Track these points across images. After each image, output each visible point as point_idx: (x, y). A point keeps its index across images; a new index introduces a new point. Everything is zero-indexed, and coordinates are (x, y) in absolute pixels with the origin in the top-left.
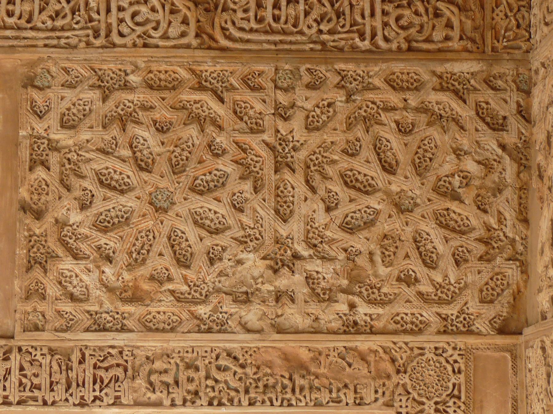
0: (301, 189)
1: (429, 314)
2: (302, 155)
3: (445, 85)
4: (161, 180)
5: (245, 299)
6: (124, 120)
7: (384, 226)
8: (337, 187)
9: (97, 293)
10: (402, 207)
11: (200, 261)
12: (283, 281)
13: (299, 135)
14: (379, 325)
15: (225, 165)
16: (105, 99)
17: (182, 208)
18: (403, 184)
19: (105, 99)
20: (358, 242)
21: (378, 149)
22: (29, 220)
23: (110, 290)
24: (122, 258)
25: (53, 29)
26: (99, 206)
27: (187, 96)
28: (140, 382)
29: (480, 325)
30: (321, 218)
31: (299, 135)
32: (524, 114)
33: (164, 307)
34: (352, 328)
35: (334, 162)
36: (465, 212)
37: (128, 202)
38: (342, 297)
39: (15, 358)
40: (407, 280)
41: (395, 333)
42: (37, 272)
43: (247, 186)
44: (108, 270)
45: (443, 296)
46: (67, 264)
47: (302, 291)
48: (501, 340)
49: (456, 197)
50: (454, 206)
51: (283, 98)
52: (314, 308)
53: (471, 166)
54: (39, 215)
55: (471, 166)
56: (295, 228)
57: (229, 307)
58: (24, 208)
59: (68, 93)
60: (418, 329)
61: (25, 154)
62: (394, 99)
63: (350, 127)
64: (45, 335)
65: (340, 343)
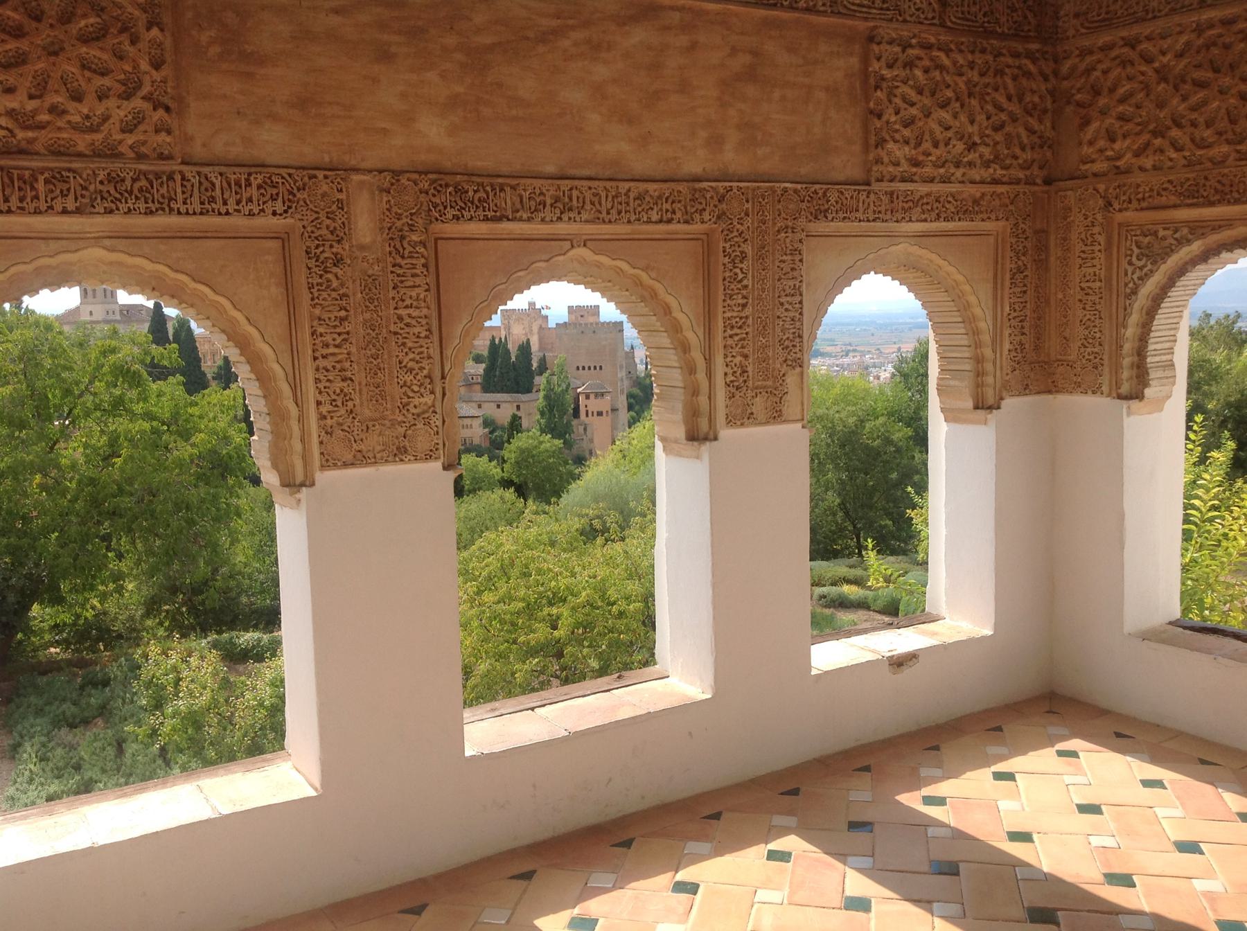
0: (978, 108)
1: (1021, 175)
2: (977, 89)
3: (1030, 56)
4: (927, 101)
5: (957, 165)
6: (909, 65)
7: (1007, 129)
8: (989, 107)
9: (903, 161)
10: (1014, 120)
11: (941, 145)
12: (971, 156)
13: (976, 78)
14: (1004, 180)
16: (903, 51)
17: (934, 116)
18: (1014, 108)
19: (903, 51)
20: (999, 137)
21: (1006, 88)
22: (876, 120)
23: (907, 160)
24: (913, 142)
25: (882, 9)
26: (902, 113)
27: (935, 53)
28: (919, 209)
29: (1039, 181)
30: (985, 123)
31: (976, 78)
32: (1056, 74)
33: (928, 170)
34: (995, 182)
35: (988, 94)
36: (1033, 122)
37: (914, 111)
38: (993, 165)
39: (872, 196)
40: (1016, 158)
41: (1010, 183)
42: (880, 149)
43: (958, 105)
44: (907, 149)
45: (1026, 166)
46: (890, 145)
48: (1046, 188)
49: (1031, 115)
50: (1030, 119)
51: (970, 57)
52: (982, 171)
53: (1036, 99)
54: (879, 116)
55: (1036, 99)
56: (976, 127)
57: (952, 170)
58: (871, 112)
59: (888, 47)
60: (1018, 182)
61: (872, 81)
62: (1010, 61)
63: (995, 75)
64: (885, 184)
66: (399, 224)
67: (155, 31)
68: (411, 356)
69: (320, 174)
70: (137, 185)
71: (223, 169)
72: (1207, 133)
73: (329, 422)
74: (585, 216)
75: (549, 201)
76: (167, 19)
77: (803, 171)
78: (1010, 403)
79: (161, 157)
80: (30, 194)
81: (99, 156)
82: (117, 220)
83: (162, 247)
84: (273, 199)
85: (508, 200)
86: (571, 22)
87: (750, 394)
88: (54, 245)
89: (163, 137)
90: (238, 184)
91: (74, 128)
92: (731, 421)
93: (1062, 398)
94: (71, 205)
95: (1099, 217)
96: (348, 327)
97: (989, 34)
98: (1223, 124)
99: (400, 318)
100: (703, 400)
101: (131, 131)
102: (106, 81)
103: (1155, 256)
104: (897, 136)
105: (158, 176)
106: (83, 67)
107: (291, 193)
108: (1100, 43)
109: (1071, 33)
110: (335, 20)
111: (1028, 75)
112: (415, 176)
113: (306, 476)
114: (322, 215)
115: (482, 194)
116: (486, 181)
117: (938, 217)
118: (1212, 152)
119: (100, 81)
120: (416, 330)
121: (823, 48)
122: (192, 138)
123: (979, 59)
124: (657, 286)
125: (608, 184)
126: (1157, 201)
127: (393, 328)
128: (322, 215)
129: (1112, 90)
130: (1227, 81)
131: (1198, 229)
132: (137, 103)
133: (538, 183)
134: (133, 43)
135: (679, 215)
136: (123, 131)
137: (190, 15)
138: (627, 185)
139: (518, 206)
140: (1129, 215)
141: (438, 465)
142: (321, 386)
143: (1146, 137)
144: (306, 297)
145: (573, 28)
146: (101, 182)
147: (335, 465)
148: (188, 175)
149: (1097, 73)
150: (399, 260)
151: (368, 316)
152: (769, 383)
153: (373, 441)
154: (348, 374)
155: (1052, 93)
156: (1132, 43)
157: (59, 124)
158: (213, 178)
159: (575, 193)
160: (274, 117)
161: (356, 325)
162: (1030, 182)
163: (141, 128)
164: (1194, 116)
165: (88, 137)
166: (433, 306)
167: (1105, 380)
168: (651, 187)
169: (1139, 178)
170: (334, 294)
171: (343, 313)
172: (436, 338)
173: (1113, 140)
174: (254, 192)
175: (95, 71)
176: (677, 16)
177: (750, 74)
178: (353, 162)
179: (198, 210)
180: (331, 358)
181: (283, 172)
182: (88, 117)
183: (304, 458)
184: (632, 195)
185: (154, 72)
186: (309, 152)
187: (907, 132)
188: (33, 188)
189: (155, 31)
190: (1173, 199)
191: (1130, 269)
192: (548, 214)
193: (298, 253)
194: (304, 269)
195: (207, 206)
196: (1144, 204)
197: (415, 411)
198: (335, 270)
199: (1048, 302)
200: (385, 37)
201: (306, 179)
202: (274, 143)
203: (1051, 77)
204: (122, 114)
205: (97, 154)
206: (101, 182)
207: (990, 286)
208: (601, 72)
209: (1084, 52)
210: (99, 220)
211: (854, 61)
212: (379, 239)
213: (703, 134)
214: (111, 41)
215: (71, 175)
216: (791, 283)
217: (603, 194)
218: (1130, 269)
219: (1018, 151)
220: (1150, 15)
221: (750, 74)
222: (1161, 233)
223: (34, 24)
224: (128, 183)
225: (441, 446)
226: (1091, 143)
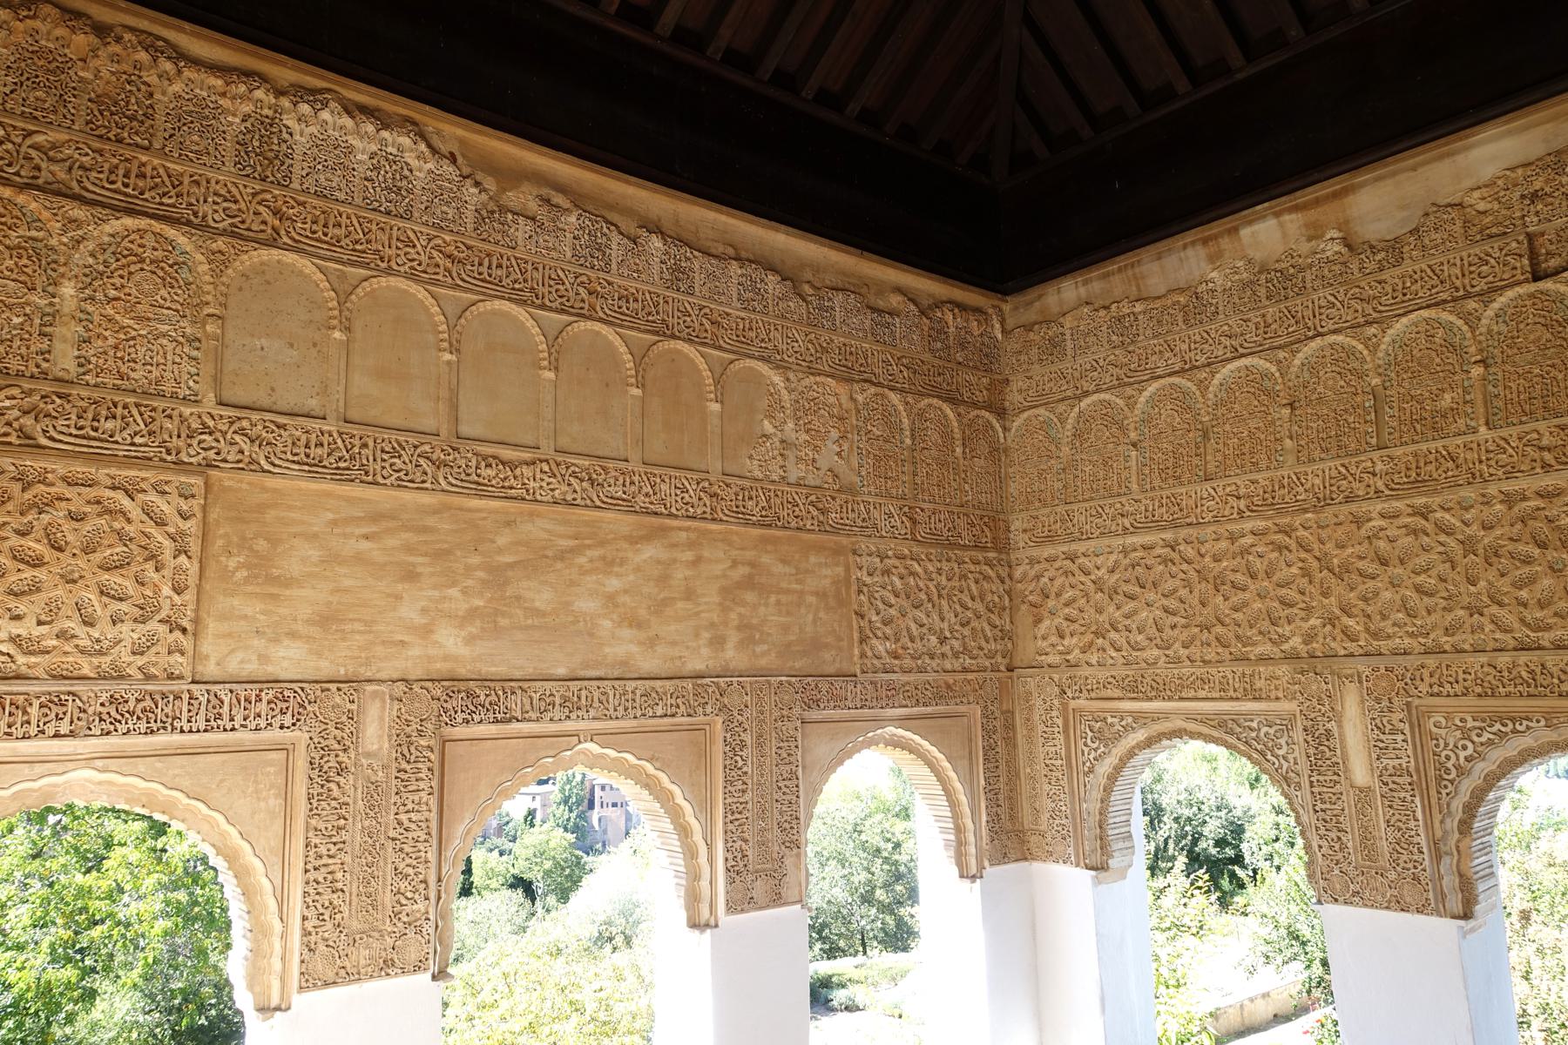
13: (944, 581)
15: (924, 597)
20: (966, 631)
27: (909, 562)
30: (953, 620)
31: (944, 581)
33: (908, 662)
34: (965, 670)
40: (981, 648)
45: (991, 655)
46: (874, 641)
47: (949, 654)
54: (862, 617)
57: (928, 661)
61: (854, 588)
62: (972, 568)
65: (961, 676)
66: (408, 730)
67: (183, 558)
68: (408, 861)
69: (333, 687)
70: (140, 706)
71: (234, 686)
72: (1140, 638)
73: (313, 938)
74: (592, 713)
75: (558, 701)
76: (194, 547)
77: (797, 665)
78: (989, 871)
79: (171, 677)
80: (20, 718)
81: (105, 678)
82: (114, 741)
83: (159, 765)
84: (283, 713)
85: (516, 704)
86: (587, 542)
87: (750, 877)
88: (38, 769)
89: (178, 657)
90: (247, 700)
91: (82, 652)
92: (731, 908)
93: (1036, 866)
94: (64, 728)
95: (1056, 702)
96: (344, 835)
97: (953, 546)
98: (1153, 631)
99: (400, 823)
100: (704, 884)
101: (142, 654)
102: (124, 606)
103: (1106, 738)
104: (879, 634)
105: (164, 696)
106: (102, 592)
107: (301, 706)
108: (1046, 555)
109: (1021, 544)
110: (365, 545)
111: (987, 578)
112: (429, 684)
113: (282, 999)
114: (331, 727)
115: (493, 698)
116: (498, 685)
117: (917, 704)
118: (1144, 655)
119: (116, 606)
120: (415, 835)
121: (813, 559)
122: (207, 657)
123: (945, 566)
124: (661, 775)
125: (616, 683)
126: (1104, 693)
127: (392, 834)
128: (331, 727)
129: (1058, 595)
130: (1151, 596)
131: (1140, 718)
132: (153, 625)
133: (548, 685)
134: (157, 570)
135: (683, 708)
136: (134, 653)
137: (220, 542)
138: (633, 684)
139: (528, 707)
140: (1081, 703)
141: (428, 975)
142: (309, 900)
143: (1089, 637)
144: (302, 807)
145: (589, 547)
146: (102, 705)
147: (315, 985)
148: (196, 694)
149: (1045, 580)
150: (404, 765)
151: (367, 823)
152: (769, 866)
153: (361, 955)
154: (339, 885)
155: (1009, 593)
156: (1072, 558)
157: (67, 648)
158: (222, 695)
159: (584, 693)
160: (293, 635)
161: (354, 835)
162: (995, 670)
163: (154, 650)
164: (1128, 622)
165: (95, 661)
166: (435, 809)
167: (1071, 850)
168: (658, 683)
169: (1085, 671)
170: (334, 803)
171: (342, 822)
172: (435, 842)
173: (1062, 637)
174: (263, 707)
175: (113, 597)
176: (684, 535)
177: (748, 583)
178: (369, 674)
179: (202, 728)
180: (323, 870)
181: (295, 686)
182: (98, 641)
183: (282, 980)
184: (638, 693)
185: (176, 597)
186: (325, 668)
187: (888, 631)
188: (25, 712)
189: (183, 558)
190: (1118, 693)
191: (1086, 750)
192: (557, 713)
193: (301, 764)
194: (306, 780)
195: (212, 723)
196: (1093, 695)
197: (405, 919)
198: (338, 779)
199: (1018, 775)
200: (411, 559)
201: (318, 693)
202: (290, 660)
203: (1007, 580)
204: (135, 636)
205: (102, 677)
206: (102, 705)
207: (966, 762)
208: (614, 584)
209: (1033, 562)
210: (93, 741)
211: (840, 570)
212: (386, 745)
213: (706, 635)
214: (134, 568)
215: (70, 698)
216: (788, 768)
217: (611, 693)
218: (1086, 750)
219: (984, 644)
220: (1085, 537)
221: (748, 583)
222: (1110, 720)
223: (60, 555)
224: (132, 704)
225: (431, 956)
226: (1044, 638)
